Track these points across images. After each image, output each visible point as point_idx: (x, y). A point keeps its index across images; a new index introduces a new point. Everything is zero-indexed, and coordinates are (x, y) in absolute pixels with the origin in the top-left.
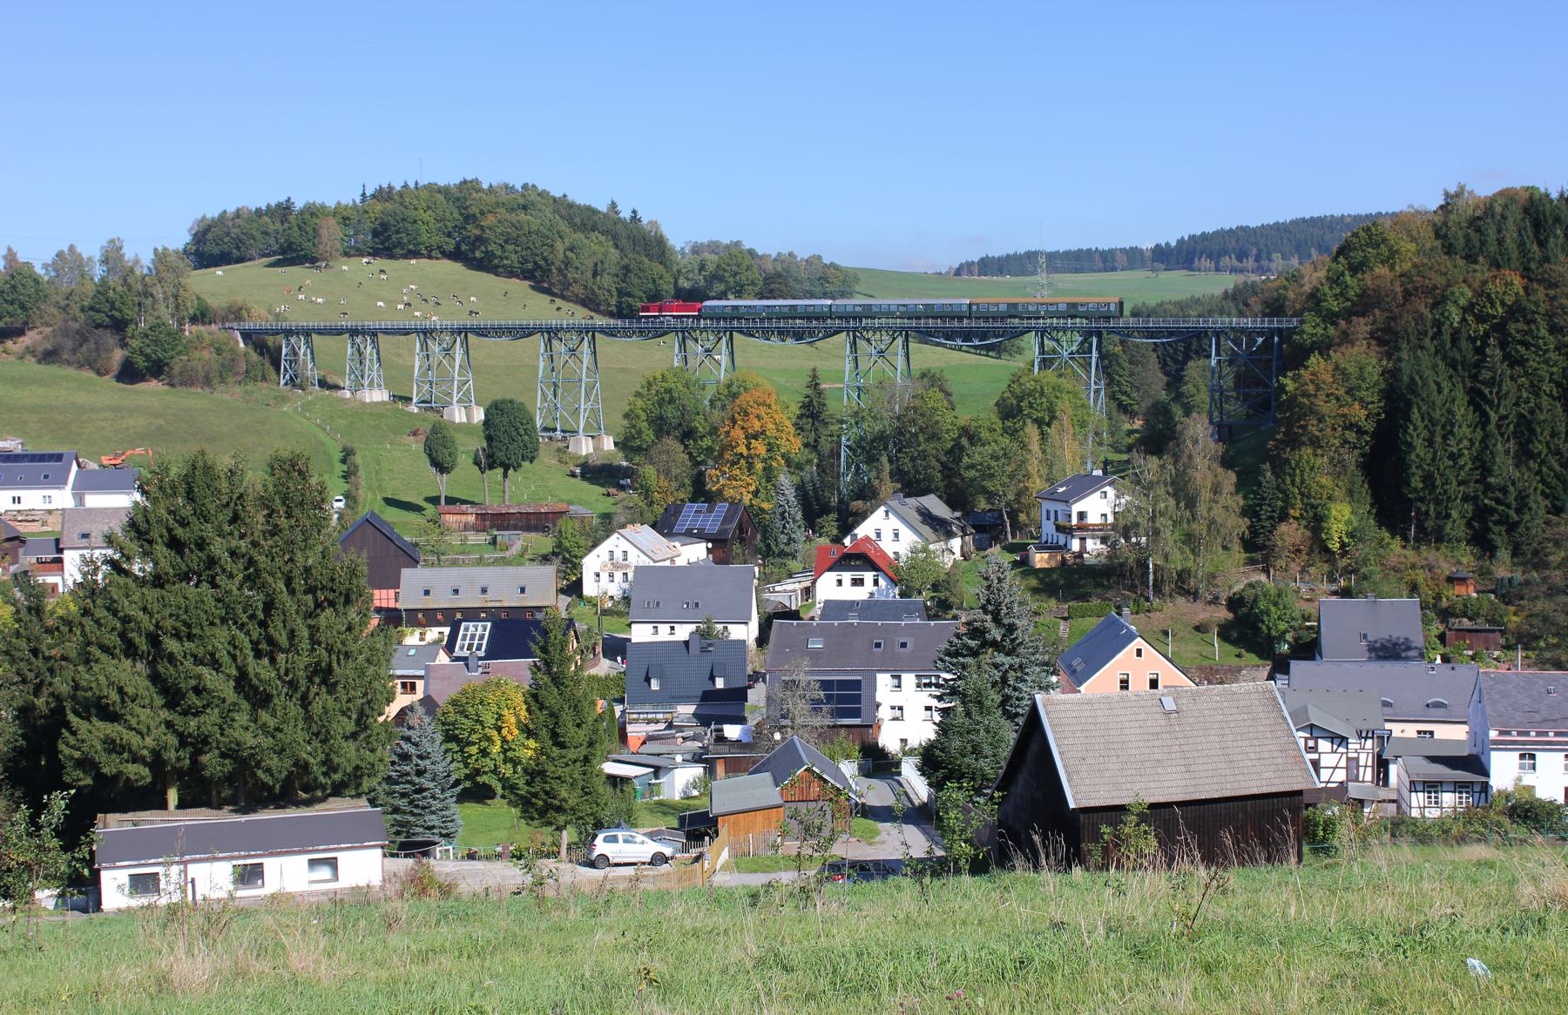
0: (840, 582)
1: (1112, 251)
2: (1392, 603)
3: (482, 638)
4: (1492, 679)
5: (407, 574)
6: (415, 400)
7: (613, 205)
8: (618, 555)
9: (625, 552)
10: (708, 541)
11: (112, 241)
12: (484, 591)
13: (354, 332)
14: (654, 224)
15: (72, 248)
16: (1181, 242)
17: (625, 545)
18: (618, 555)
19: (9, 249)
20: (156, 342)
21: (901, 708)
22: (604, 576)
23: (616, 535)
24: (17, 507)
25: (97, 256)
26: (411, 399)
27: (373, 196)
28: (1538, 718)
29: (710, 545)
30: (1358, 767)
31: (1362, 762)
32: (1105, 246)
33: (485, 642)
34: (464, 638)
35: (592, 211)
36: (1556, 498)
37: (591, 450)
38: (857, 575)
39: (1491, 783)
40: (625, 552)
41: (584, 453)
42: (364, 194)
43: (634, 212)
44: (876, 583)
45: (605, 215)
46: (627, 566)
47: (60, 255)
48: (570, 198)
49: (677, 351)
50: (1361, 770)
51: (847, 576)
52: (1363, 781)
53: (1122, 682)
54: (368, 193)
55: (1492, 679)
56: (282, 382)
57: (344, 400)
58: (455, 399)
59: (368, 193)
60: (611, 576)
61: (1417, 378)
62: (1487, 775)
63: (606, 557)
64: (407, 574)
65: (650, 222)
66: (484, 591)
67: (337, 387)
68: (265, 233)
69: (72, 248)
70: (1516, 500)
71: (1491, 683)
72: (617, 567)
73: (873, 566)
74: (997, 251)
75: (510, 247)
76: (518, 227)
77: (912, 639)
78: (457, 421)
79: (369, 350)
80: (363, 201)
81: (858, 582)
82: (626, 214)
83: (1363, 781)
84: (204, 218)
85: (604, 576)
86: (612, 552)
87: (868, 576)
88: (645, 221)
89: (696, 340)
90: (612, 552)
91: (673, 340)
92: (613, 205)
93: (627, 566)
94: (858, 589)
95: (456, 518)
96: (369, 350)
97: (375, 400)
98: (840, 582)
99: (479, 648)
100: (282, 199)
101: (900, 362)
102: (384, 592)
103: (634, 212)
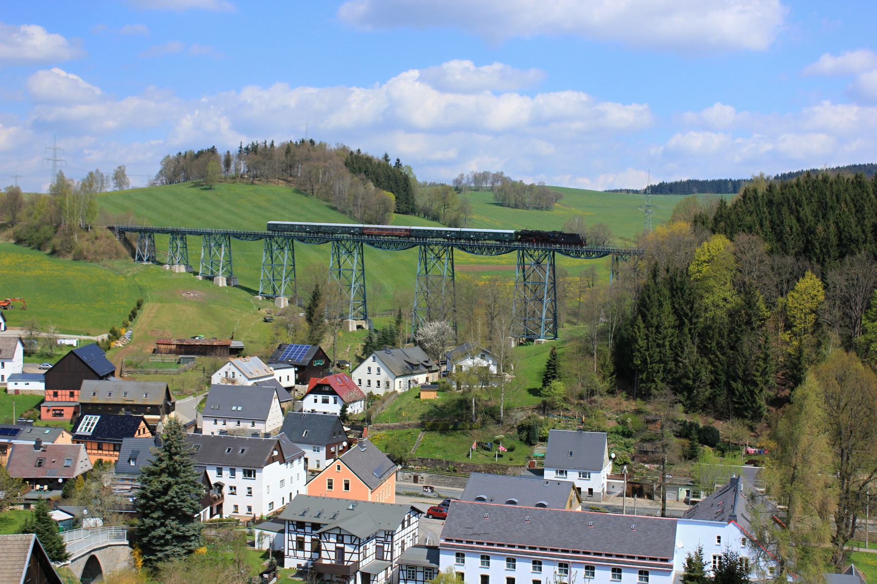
0: (316, 401)
1: (739, 181)
2: (591, 434)
3: (93, 424)
4: (456, 506)
5: (86, 383)
7: (386, 157)
8: (230, 374)
9: (233, 373)
10: (295, 366)
11: (120, 167)
12: (126, 394)
13: (174, 233)
14: (409, 168)
15: (97, 171)
17: (233, 369)
18: (230, 374)
19: (60, 171)
21: (235, 488)
25: (112, 176)
27: (247, 149)
28: (471, 532)
29: (296, 369)
30: (384, 551)
31: (386, 549)
33: (93, 428)
34: (93, 424)
35: (369, 160)
36: (718, 375)
39: (440, 569)
40: (233, 373)
41: (282, 306)
42: (241, 147)
43: (398, 160)
45: (379, 164)
47: (91, 174)
48: (363, 152)
50: (385, 553)
51: (320, 397)
52: (386, 560)
53: (329, 484)
54: (243, 147)
55: (456, 506)
57: (165, 272)
58: (221, 273)
59: (243, 147)
61: (647, 299)
62: (438, 564)
64: (86, 383)
65: (407, 166)
66: (126, 394)
67: (162, 264)
69: (97, 171)
71: (455, 508)
73: (333, 392)
74: (670, 180)
77: (248, 448)
78: (220, 285)
80: (240, 151)
81: (325, 401)
82: (392, 163)
83: (386, 560)
84: (168, 156)
86: (226, 373)
87: (331, 398)
88: (403, 165)
90: (226, 373)
91: (328, 247)
92: (386, 157)
95: (164, 346)
96: (179, 243)
98: (316, 401)
99: (89, 431)
100: (210, 147)
103: (398, 160)
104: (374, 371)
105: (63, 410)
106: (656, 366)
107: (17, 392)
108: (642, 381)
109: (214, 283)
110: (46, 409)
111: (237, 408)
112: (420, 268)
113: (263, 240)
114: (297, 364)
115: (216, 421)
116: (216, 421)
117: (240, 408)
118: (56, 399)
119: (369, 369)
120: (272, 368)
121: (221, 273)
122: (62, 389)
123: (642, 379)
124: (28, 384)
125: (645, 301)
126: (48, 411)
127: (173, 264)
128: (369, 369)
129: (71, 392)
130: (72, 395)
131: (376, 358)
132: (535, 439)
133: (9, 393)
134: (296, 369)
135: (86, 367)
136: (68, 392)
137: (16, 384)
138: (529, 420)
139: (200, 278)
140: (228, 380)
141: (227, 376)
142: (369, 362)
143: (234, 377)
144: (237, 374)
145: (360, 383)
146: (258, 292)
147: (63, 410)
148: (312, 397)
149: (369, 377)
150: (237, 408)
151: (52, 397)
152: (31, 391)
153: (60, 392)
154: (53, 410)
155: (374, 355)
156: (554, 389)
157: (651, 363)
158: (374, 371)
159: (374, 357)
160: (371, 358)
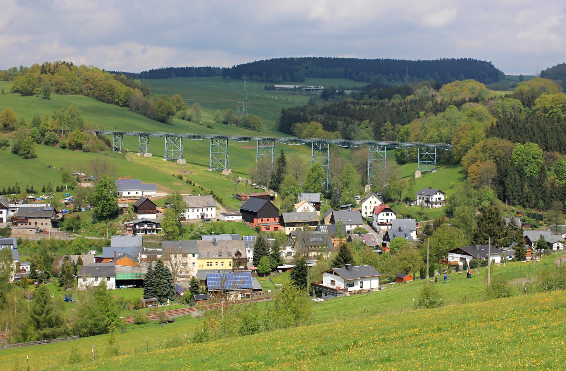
1: (199, 68)
8: (306, 208)
16: (234, 67)
18: (306, 208)
24: (129, 195)
32: (197, 65)
44: (391, 215)
51: (385, 213)
63: (303, 208)
81: (387, 214)
87: (390, 213)
104: (373, 202)
107: (228, 221)
119: (371, 202)
128: (371, 202)
130: (268, 220)
136: (267, 219)
140: (306, 210)
148: (382, 214)
149: (371, 205)
153: (263, 219)
158: (373, 202)
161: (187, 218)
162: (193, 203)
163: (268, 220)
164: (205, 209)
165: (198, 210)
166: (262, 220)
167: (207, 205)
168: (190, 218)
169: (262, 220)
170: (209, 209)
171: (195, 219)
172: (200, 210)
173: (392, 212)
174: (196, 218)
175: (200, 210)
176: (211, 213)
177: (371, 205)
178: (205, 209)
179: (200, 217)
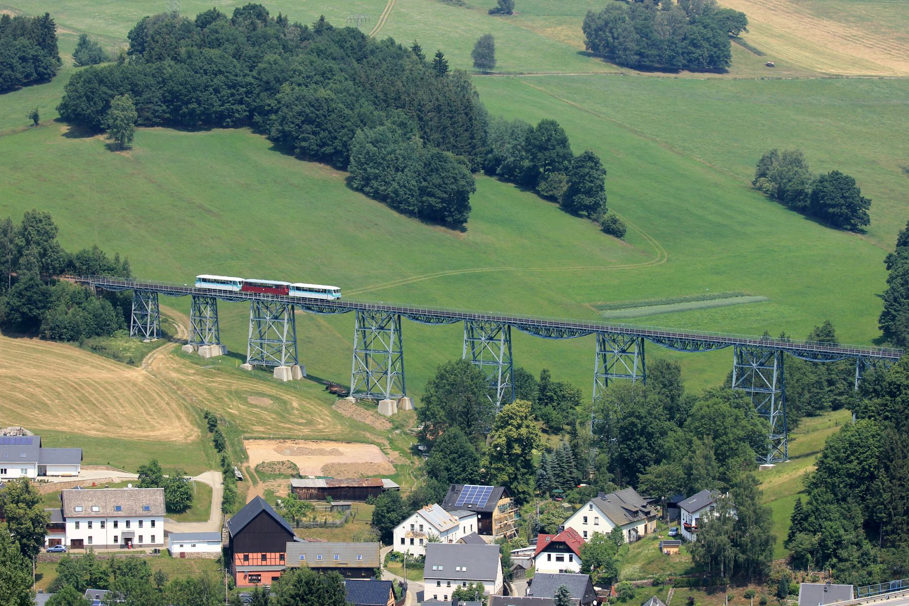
2: (838, 587)
6: (249, 358)
8: (417, 527)
9: (421, 526)
10: (478, 513)
17: (421, 521)
18: (417, 527)
20: (30, 301)
22: (408, 541)
23: (416, 515)
26: (246, 357)
37: (396, 411)
38: (560, 555)
40: (421, 526)
43: (439, 55)
44: (571, 560)
46: (423, 535)
49: (465, 337)
51: (554, 555)
56: (132, 333)
58: (283, 362)
60: (412, 541)
63: (409, 528)
68: (23, 59)
70: (808, 560)
72: (416, 535)
73: (568, 550)
75: (306, 127)
76: (315, 104)
79: (208, 312)
81: (560, 559)
85: (408, 541)
86: (412, 526)
87: (566, 556)
89: (482, 328)
90: (412, 526)
93: (423, 535)
94: (560, 563)
96: (208, 312)
97: (213, 355)
101: (637, 360)
102: (273, 554)
104: (591, 520)
105: (260, 575)
106: (899, 519)
107: (182, 555)
108: (887, 533)
109: (275, 376)
110: (243, 575)
111: (461, 569)
112: (598, 365)
113: (354, 313)
114: (480, 510)
115: (439, 584)
116: (439, 584)
117: (464, 569)
118: (246, 563)
119: (586, 519)
120: (457, 518)
121: (284, 359)
122: (271, 552)
123: (886, 531)
124: (194, 546)
125: (888, 453)
126: (245, 577)
127: (202, 343)
128: (586, 519)
129: (262, 555)
130: (264, 558)
131: (594, 506)
132: (785, 593)
133: (174, 556)
134: (479, 516)
135: (279, 527)
136: (260, 555)
137: (182, 546)
138: (777, 575)
139: (248, 366)
141: (413, 530)
142: (585, 511)
143: (421, 530)
144: (426, 527)
145: (586, 536)
146: (349, 389)
147: (260, 575)
148: (545, 554)
149: (585, 528)
150: (461, 569)
151: (242, 561)
152: (198, 553)
153: (251, 555)
154: (250, 575)
155: (590, 503)
156: (802, 544)
157: (895, 515)
159: (591, 506)
160: (587, 507)
161: (86, 543)
162: (105, 507)
163: (264, 558)
164: (134, 525)
165: (116, 525)
166: (246, 558)
167: (141, 511)
168: (94, 542)
169: (246, 558)
170: (147, 524)
171: (107, 547)
172: (122, 525)
173: (572, 552)
174: (111, 542)
175: (122, 525)
176: (153, 531)
177: (585, 528)
178: (134, 525)
179: (120, 542)
